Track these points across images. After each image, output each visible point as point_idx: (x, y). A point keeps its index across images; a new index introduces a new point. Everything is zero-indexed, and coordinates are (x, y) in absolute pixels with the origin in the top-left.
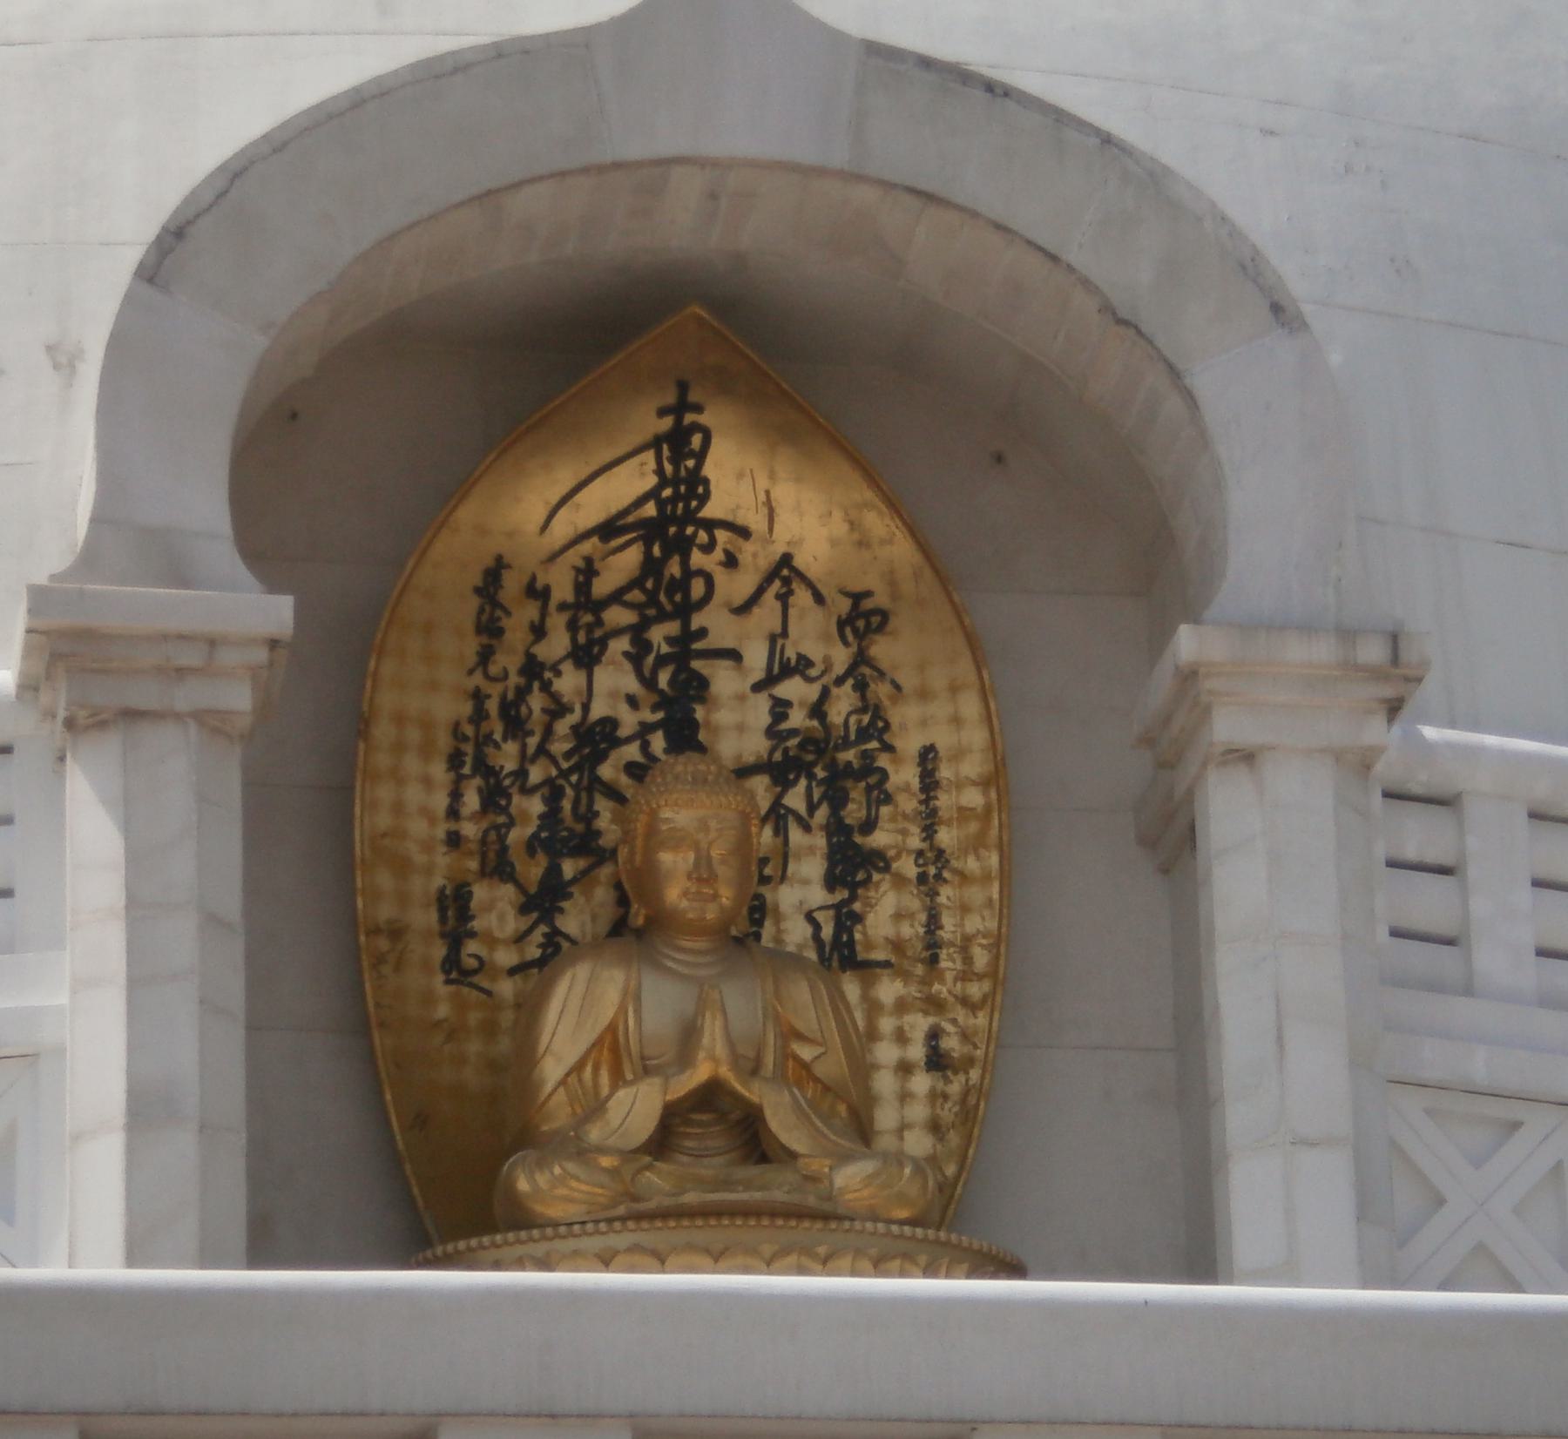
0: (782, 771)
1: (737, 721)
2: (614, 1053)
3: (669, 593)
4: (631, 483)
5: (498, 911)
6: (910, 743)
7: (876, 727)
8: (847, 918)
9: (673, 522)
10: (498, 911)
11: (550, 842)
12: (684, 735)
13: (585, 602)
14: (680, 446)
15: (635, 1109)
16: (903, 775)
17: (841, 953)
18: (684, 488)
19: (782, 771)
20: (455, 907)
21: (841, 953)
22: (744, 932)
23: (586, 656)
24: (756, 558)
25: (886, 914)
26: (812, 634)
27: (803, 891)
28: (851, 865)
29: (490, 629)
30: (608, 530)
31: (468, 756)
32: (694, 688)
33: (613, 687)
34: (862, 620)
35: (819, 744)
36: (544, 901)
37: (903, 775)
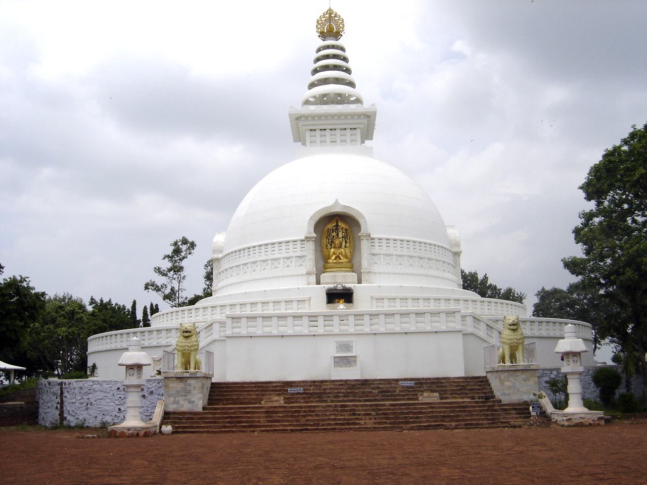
0: (343, 238)
1: (340, 235)
2: (334, 254)
3: (337, 229)
5: (329, 245)
6: (349, 236)
7: (347, 235)
9: (337, 226)
10: (329, 245)
11: (331, 242)
13: (333, 230)
14: (337, 222)
16: (348, 238)
17: (346, 247)
18: (337, 224)
20: (327, 245)
23: (333, 232)
24: (341, 227)
25: (348, 244)
26: (344, 231)
27: (344, 244)
28: (346, 242)
29: (328, 231)
30: (334, 226)
31: (327, 238)
32: (338, 234)
34: (346, 230)
36: (331, 245)
37: (348, 238)
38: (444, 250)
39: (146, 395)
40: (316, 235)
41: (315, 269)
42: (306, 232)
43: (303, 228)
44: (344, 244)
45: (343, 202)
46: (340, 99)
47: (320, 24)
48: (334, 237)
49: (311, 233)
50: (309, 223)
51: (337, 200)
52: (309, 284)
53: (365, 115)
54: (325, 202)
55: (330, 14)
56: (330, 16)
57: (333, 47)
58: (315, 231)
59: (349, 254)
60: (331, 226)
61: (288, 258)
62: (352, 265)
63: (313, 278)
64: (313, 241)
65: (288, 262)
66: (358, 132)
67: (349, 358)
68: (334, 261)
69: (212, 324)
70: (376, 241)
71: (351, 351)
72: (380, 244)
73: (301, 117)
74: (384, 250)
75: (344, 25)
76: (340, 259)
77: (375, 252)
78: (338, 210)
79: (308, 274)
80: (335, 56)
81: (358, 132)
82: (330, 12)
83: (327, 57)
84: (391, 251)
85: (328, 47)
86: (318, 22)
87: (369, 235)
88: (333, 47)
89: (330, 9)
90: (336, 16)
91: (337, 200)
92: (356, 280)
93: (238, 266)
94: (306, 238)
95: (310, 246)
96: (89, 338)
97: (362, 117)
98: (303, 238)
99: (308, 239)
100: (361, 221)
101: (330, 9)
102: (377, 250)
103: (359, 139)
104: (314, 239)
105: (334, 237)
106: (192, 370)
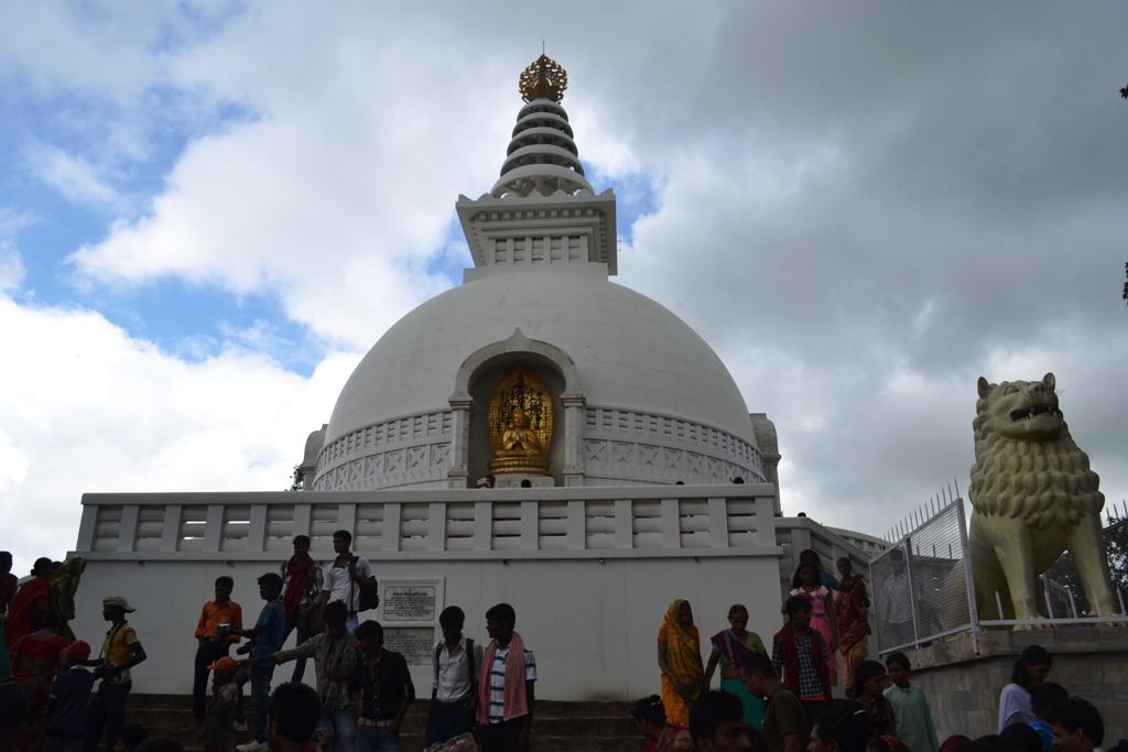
1: (527, 405)
2: (510, 439)
4: (516, 382)
5: (503, 425)
7: (541, 404)
8: (538, 424)
10: (503, 425)
12: (522, 406)
13: (513, 394)
15: (510, 445)
19: (532, 409)
20: (499, 426)
21: (537, 428)
22: (525, 425)
23: (512, 399)
25: (542, 423)
27: (534, 421)
28: (538, 419)
31: (500, 409)
34: (539, 394)
35: (536, 406)
36: (508, 424)
38: (744, 447)
40: (471, 399)
41: (466, 467)
42: (452, 392)
44: (534, 421)
45: (530, 333)
46: (550, 185)
47: (525, 80)
48: (514, 407)
49: (461, 394)
51: (518, 329)
53: (595, 210)
57: (546, 109)
58: (472, 391)
64: (466, 410)
65: (416, 455)
66: (583, 241)
67: (411, 633)
68: (511, 453)
70: (600, 414)
71: (428, 612)
72: (607, 421)
73: (477, 215)
74: (615, 432)
75: (566, 80)
76: (523, 449)
77: (593, 434)
80: (548, 123)
81: (583, 241)
82: (543, 60)
84: (630, 434)
86: (522, 76)
87: (583, 400)
88: (546, 109)
89: (543, 57)
90: (554, 66)
91: (518, 329)
95: (458, 420)
97: (590, 212)
98: (448, 406)
100: (567, 371)
101: (543, 57)
102: (599, 432)
104: (468, 407)
105: (514, 407)
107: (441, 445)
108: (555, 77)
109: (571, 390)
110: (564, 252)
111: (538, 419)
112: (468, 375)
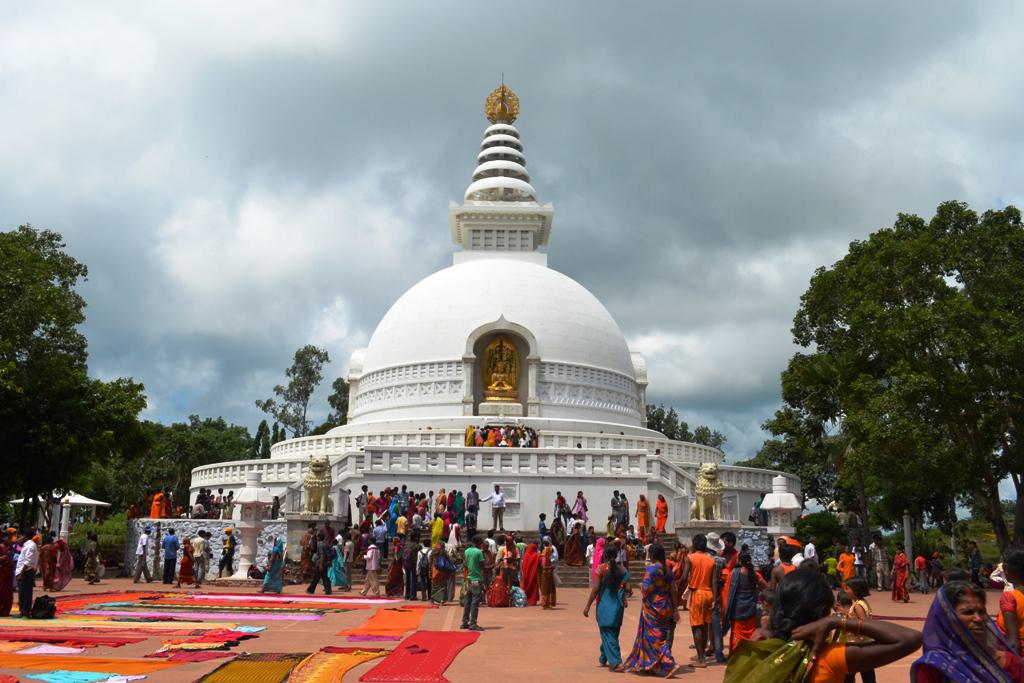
1: (505, 358)
3: (501, 350)
4: (498, 344)
9: (501, 346)
14: (501, 342)
21: (510, 372)
22: (504, 372)
25: (513, 369)
27: (508, 368)
28: (511, 367)
33: (497, 356)
34: (512, 352)
39: (264, 541)
40: (475, 356)
41: (472, 397)
43: (461, 349)
45: (510, 318)
50: (468, 342)
52: (464, 414)
54: (487, 316)
55: (503, 92)
56: (503, 95)
59: (514, 381)
60: (492, 347)
61: (440, 383)
62: (518, 395)
63: (470, 407)
65: (441, 387)
66: (530, 236)
69: (346, 458)
78: (503, 327)
79: (464, 402)
83: (497, 143)
84: (564, 378)
85: (499, 132)
86: (488, 100)
87: (539, 360)
88: (505, 132)
89: (503, 87)
92: (521, 413)
93: (379, 390)
94: (464, 359)
96: (193, 471)
99: (466, 360)
100: (530, 342)
103: (530, 242)
106: (322, 512)
107: (456, 382)
108: (511, 106)
109: (532, 355)
110: (518, 242)
111: (511, 367)
112: (473, 342)
